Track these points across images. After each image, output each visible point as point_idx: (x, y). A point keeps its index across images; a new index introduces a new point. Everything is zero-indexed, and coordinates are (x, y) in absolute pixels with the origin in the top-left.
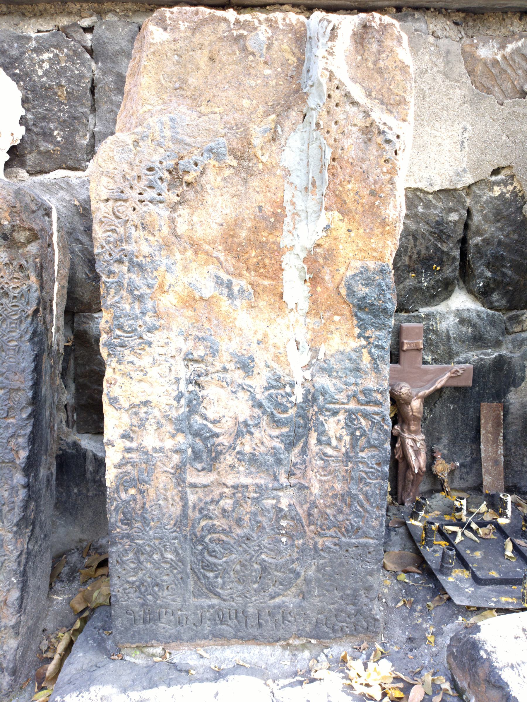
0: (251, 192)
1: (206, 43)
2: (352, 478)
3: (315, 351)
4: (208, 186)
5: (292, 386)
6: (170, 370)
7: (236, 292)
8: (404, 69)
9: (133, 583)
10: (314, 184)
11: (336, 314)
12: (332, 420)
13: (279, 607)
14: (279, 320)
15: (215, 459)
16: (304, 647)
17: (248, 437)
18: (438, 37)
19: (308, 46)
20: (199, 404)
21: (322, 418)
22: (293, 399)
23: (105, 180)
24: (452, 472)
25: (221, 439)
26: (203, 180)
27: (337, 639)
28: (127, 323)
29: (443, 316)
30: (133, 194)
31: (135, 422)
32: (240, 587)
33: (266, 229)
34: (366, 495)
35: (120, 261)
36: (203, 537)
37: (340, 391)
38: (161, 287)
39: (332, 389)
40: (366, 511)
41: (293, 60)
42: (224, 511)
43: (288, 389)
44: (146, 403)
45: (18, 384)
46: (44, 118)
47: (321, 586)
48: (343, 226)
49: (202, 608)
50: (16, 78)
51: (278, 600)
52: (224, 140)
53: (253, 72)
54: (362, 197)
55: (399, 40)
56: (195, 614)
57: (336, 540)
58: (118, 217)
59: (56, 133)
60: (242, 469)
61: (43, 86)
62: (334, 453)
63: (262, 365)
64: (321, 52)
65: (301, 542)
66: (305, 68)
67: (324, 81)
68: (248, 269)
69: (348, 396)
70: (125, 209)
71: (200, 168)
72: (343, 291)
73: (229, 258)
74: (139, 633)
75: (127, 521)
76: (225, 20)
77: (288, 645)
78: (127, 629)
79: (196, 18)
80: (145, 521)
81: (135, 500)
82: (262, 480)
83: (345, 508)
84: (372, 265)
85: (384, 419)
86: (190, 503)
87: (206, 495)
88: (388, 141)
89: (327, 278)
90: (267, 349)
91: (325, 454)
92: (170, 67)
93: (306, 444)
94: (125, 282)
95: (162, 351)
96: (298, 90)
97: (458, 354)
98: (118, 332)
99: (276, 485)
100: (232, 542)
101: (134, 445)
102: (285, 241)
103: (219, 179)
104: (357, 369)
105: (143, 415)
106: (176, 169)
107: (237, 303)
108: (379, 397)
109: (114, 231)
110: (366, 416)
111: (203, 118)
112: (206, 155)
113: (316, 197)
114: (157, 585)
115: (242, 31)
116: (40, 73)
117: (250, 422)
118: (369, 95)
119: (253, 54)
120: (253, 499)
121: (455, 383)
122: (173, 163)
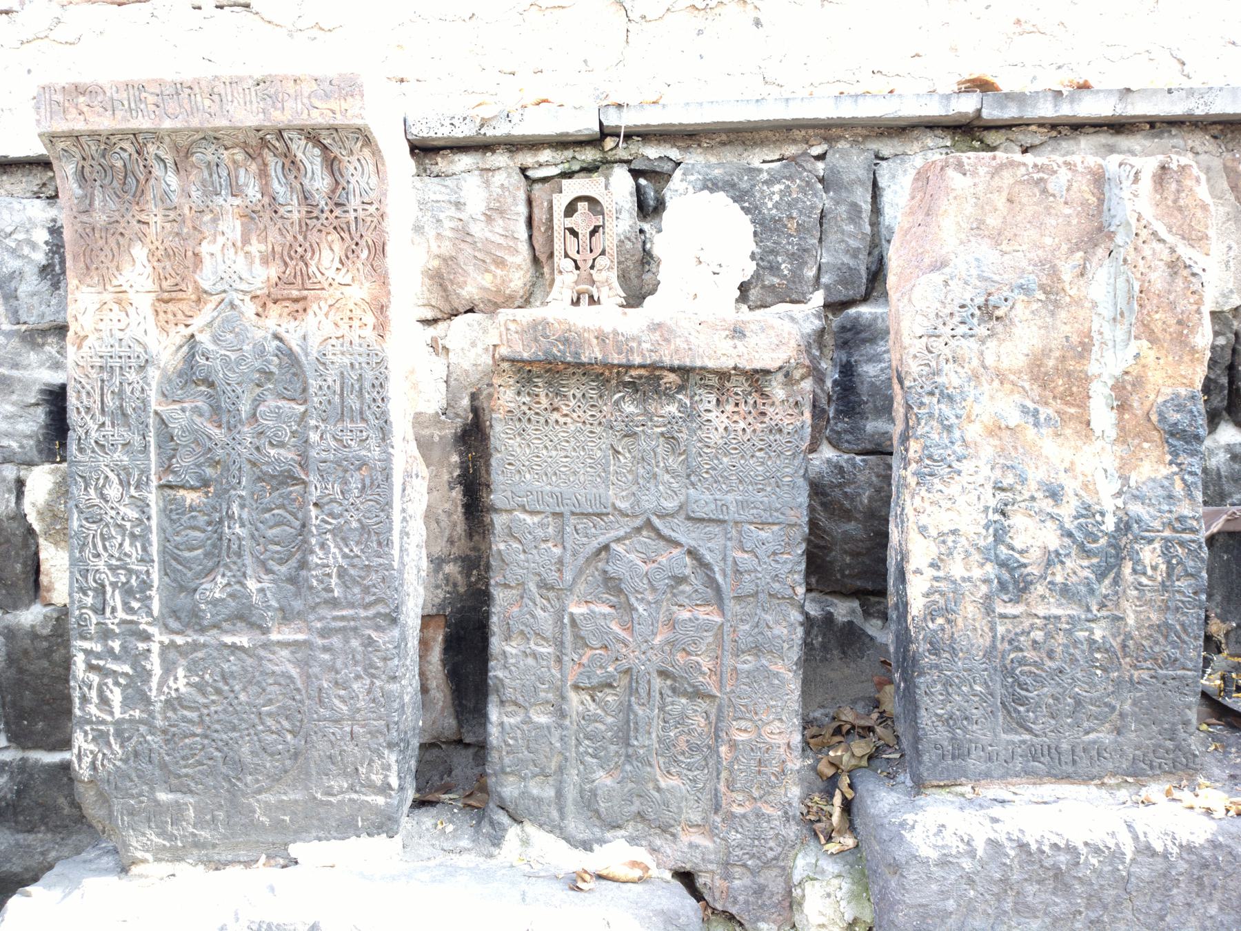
0: (1058, 322)
1: (1005, 186)
2: (1168, 608)
3: (1125, 479)
4: (1016, 320)
5: (1102, 514)
6: (979, 498)
7: (1042, 420)
8: (1205, 207)
9: (941, 716)
10: (1122, 314)
11: (1146, 441)
12: (1148, 548)
13: (1095, 742)
14: (1085, 448)
15: (1025, 590)
16: (1119, 786)
17: (1059, 567)
18: (1197, 153)
19: (1107, 186)
20: (1006, 533)
21: (1137, 547)
22: (1103, 528)
23: (919, 318)
24: (1227, 635)
25: (1029, 569)
26: (1012, 314)
27: (1155, 777)
28: (936, 453)
29: (1211, 452)
30: (946, 331)
31: (943, 550)
32: (1053, 722)
33: (1073, 358)
34: (1183, 625)
35: (931, 394)
36: (1013, 669)
37: (1154, 518)
38: (968, 417)
39: (1146, 517)
40: (1184, 642)
41: (1093, 200)
42: (1035, 642)
43: (1098, 517)
44: (954, 532)
45: (794, 520)
46: (772, 252)
47: (1138, 721)
48: (1152, 355)
49: (1014, 743)
50: (747, 211)
51: (1092, 736)
52: (1032, 277)
53: (1053, 211)
54: (1169, 326)
55: (1198, 180)
56: (1006, 749)
57: (1152, 672)
58: (930, 352)
59: (783, 266)
60: (1052, 600)
61: (773, 219)
62: (1150, 583)
63: (1071, 493)
64: (1126, 194)
65: (1116, 674)
66: (1105, 207)
67: (1133, 222)
68: (1055, 397)
69: (1163, 523)
70: (938, 344)
71: (1010, 303)
72: (1154, 418)
73: (1035, 387)
74: (948, 770)
75: (935, 650)
76: (1024, 164)
77: (1103, 784)
78: (935, 765)
79: (994, 163)
80: (954, 652)
81: (943, 630)
82: (1074, 611)
83: (1161, 639)
84: (1183, 392)
85: (1200, 547)
86: (999, 636)
87: (1014, 627)
88: (1194, 275)
89: (1135, 405)
90: (1075, 478)
91: (1140, 584)
92: (969, 209)
93: (1118, 575)
94: (936, 413)
95: (971, 479)
96: (1100, 229)
97: (1230, 495)
98: (927, 462)
99: (1090, 616)
100: (1044, 675)
101: (941, 574)
102: (1092, 368)
103: (1027, 312)
104: (1170, 497)
105: (950, 544)
106: (986, 305)
107: (1044, 431)
108: (1195, 523)
109: (928, 365)
110: (1182, 544)
111: (1007, 256)
112: (1016, 291)
113: (1125, 327)
114: (966, 718)
115: (1041, 175)
116: (770, 205)
117: (1061, 552)
118: (1170, 231)
119: (1054, 196)
120: (1066, 630)
121: (1231, 528)
122: (983, 299)
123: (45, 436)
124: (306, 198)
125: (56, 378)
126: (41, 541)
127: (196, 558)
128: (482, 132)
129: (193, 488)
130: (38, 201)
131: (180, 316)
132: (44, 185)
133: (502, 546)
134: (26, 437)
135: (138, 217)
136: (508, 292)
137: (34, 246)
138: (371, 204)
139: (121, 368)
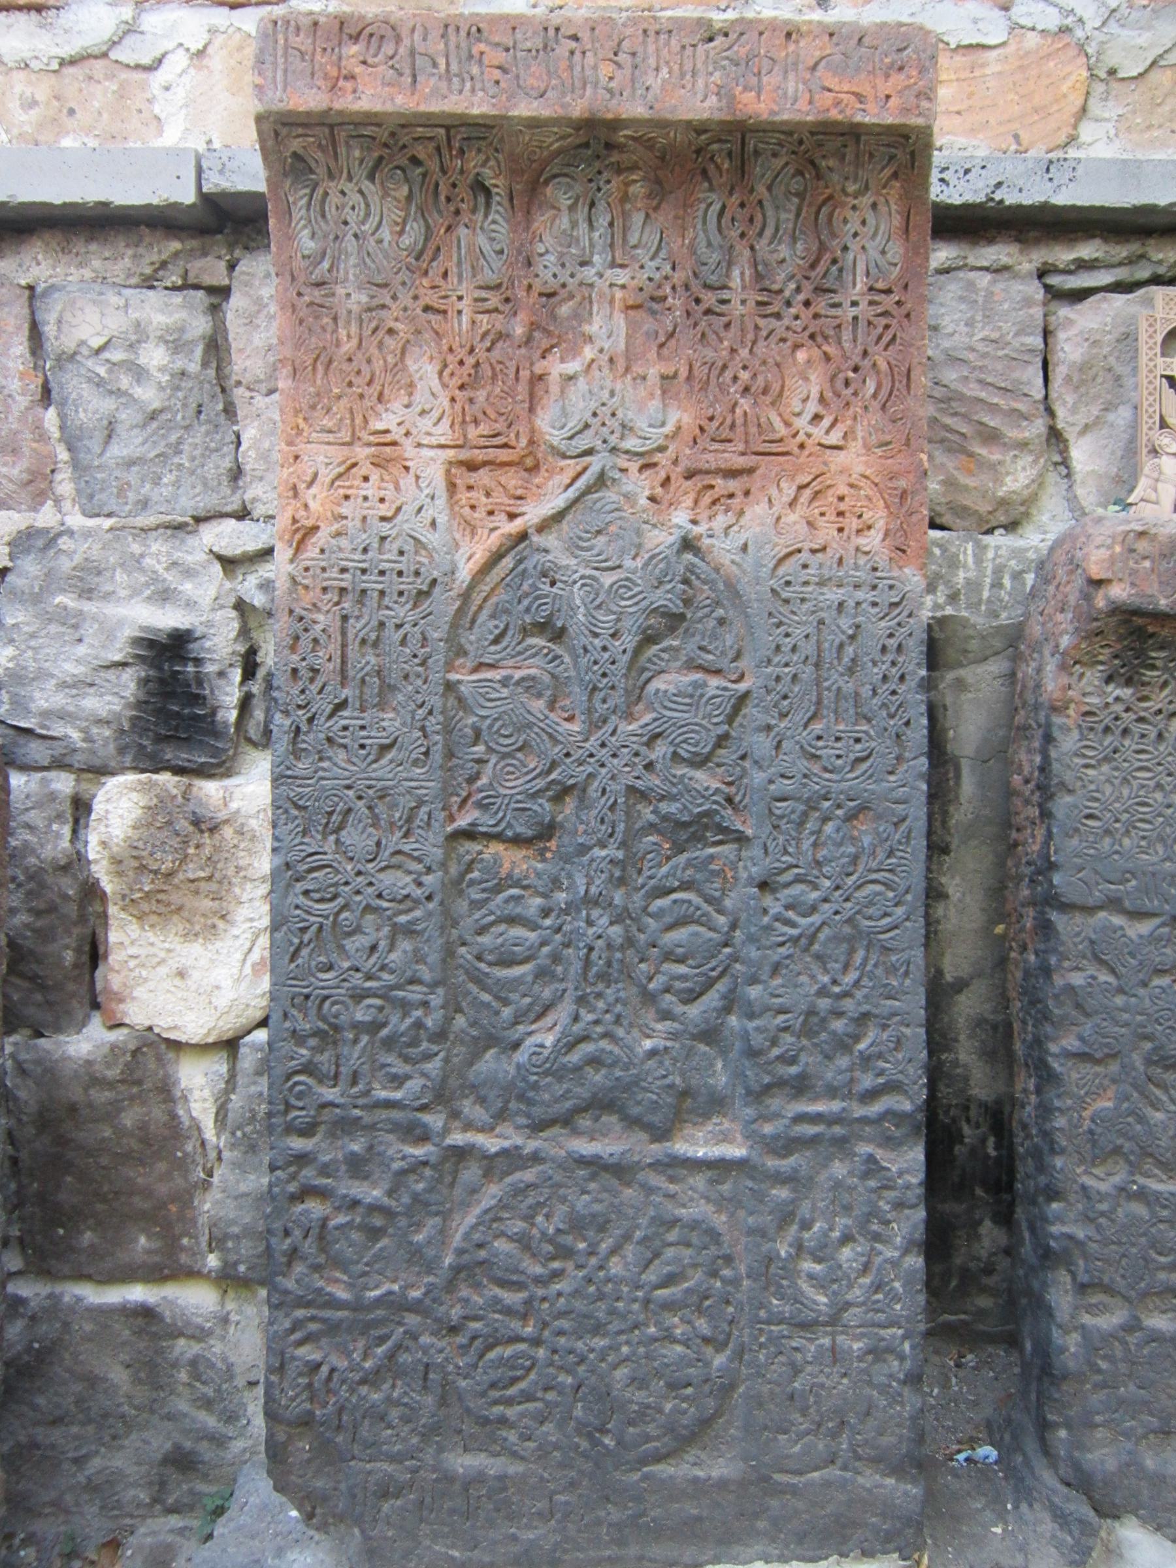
123: (133, 720)
124: (759, 277)
125: (168, 619)
126: (112, 910)
127: (519, 981)
128: (997, 196)
129: (518, 841)
130: (151, 293)
131: (499, 497)
132: (164, 265)
133: (1077, 979)
134: (100, 722)
135: (427, 300)
136: (1000, 494)
137: (140, 373)
138: (888, 291)
139: (382, 593)
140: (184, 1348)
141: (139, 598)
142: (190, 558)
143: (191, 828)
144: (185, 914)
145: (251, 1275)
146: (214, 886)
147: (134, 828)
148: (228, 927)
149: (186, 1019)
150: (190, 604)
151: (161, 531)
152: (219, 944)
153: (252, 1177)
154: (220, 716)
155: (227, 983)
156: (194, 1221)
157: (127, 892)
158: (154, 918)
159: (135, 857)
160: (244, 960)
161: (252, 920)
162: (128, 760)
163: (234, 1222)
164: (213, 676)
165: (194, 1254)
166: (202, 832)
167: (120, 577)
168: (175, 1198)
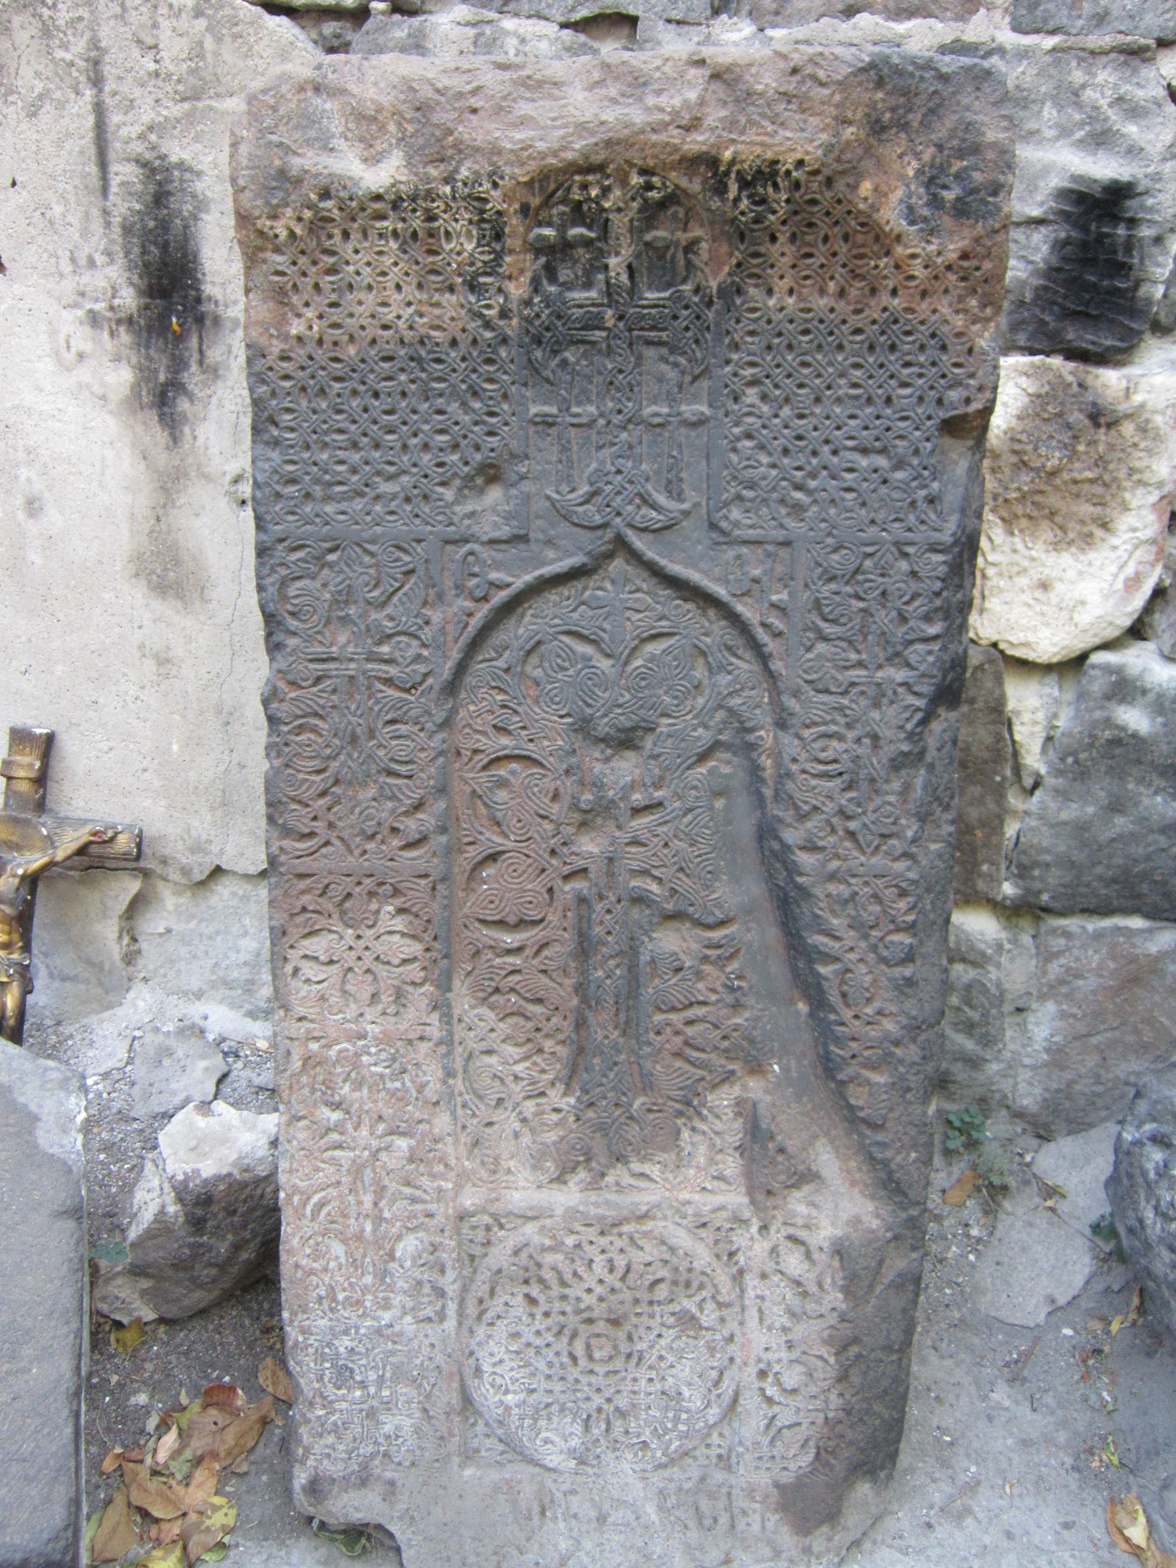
123: (1041, 294)
140: (961, 973)
141: (1068, 141)
142: (1141, 93)
143: (1087, 422)
144: (1058, 519)
145: (1052, 905)
146: (1098, 489)
147: (1019, 418)
148: (1106, 535)
149: (1040, 635)
150: (1134, 151)
151: (1113, 55)
152: (1092, 555)
153: (1074, 806)
154: (1142, 292)
155: (1094, 598)
156: (999, 846)
157: (1000, 490)
158: (1024, 522)
159: (1015, 452)
160: (1116, 576)
161: (1135, 530)
162: (1022, 339)
163: (1047, 851)
164: (1147, 241)
165: (992, 880)
166: (1097, 425)
167: (1049, 112)
168: (983, 824)
